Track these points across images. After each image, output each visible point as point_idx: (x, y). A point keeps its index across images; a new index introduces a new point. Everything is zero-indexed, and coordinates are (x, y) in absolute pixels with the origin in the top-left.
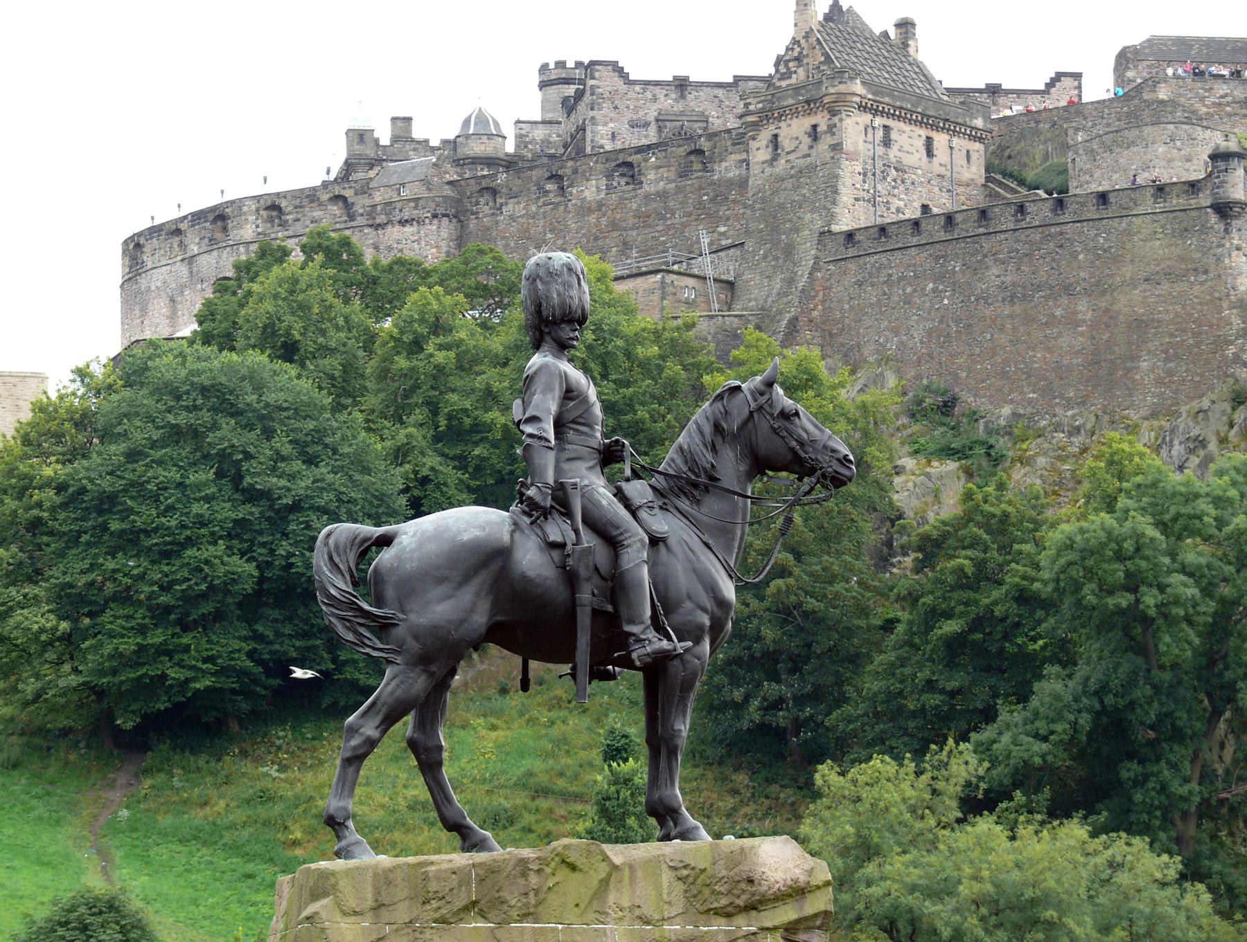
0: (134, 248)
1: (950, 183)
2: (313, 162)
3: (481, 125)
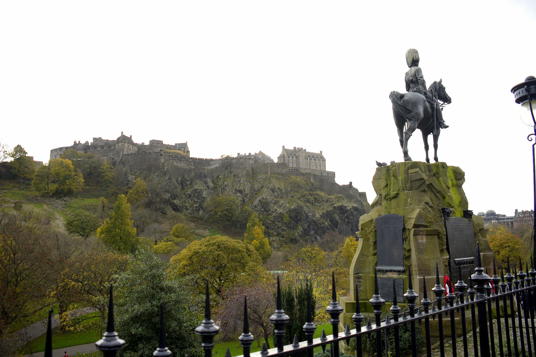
0: (52, 151)
1: (134, 151)
2: (71, 144)
3: (87, 142)
